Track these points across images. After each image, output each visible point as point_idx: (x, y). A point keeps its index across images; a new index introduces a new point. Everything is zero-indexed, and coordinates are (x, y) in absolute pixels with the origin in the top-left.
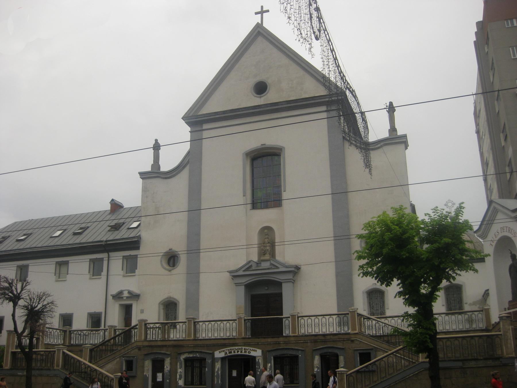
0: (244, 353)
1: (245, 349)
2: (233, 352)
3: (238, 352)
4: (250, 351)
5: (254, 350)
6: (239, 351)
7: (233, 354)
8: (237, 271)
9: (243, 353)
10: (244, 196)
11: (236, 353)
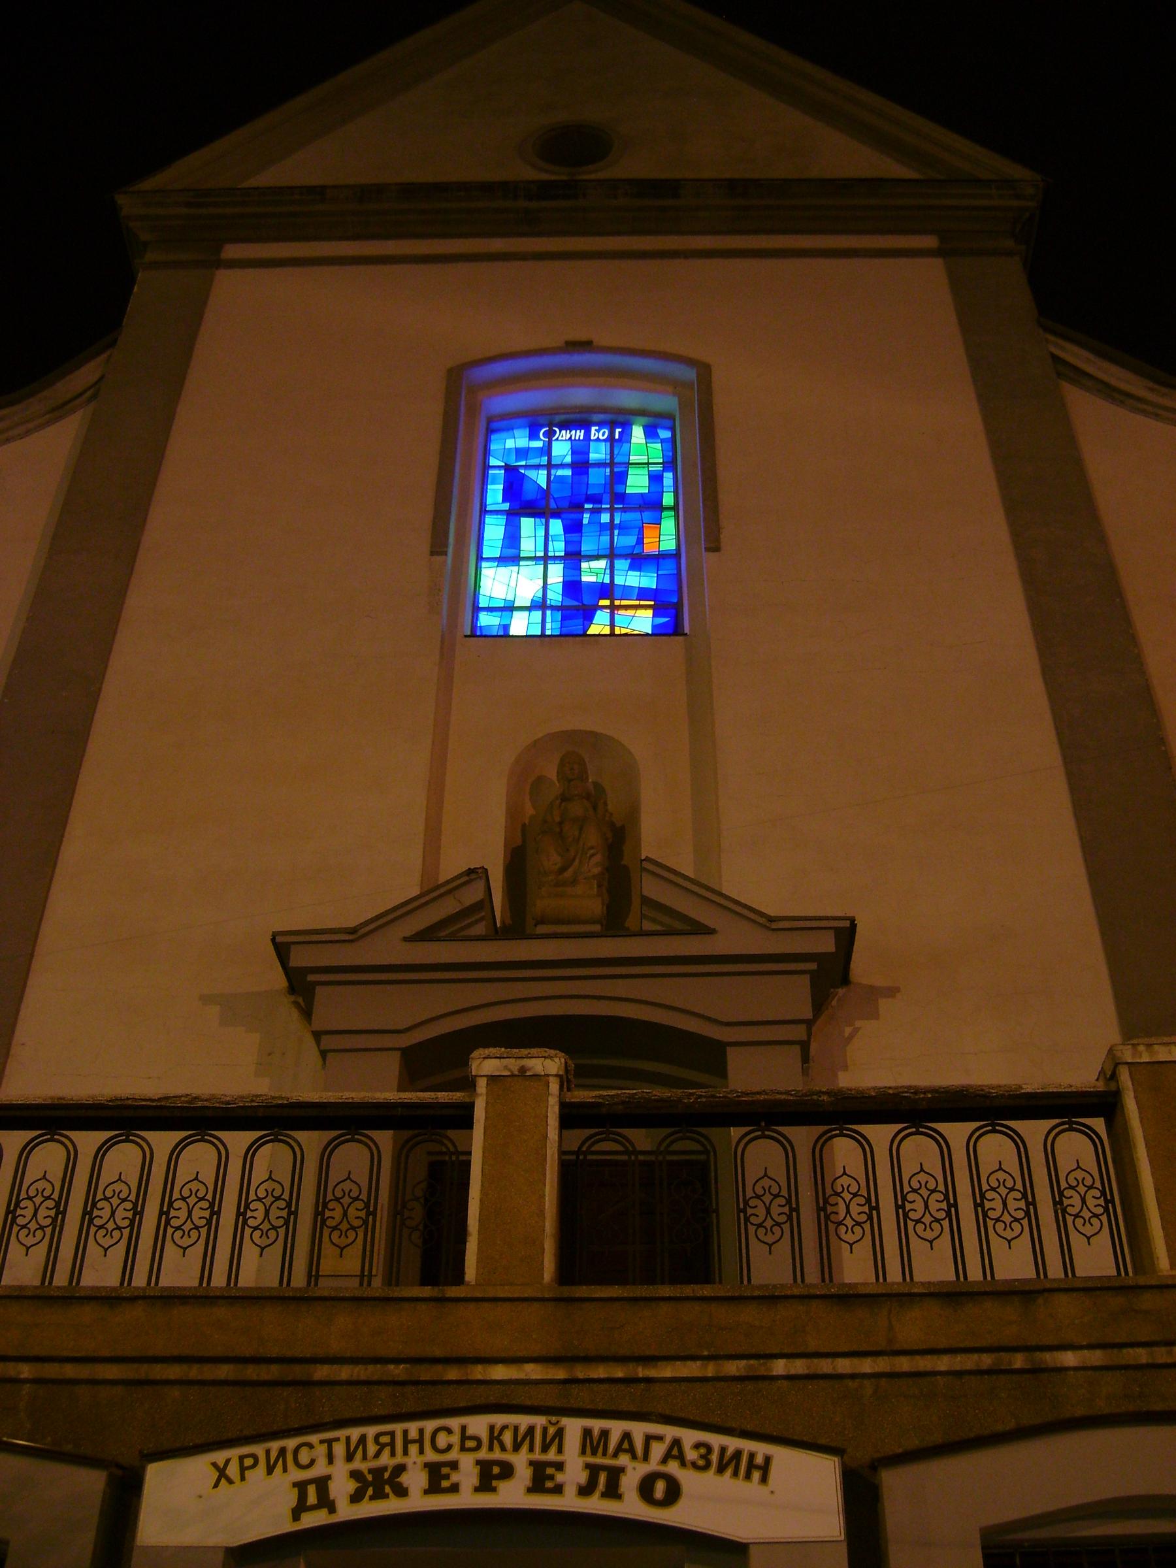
0: (585, 1491)
1: (591, 1443)
2: (415, 1479)
3: (486, 1484)
4: (673, 1467)
5: (728, 1463)
6: (507, 1471)
7: (418, 1501)
8: (354, 934)
9: (569, 1502)
10: (432, 553)
11: (467, 1499)
